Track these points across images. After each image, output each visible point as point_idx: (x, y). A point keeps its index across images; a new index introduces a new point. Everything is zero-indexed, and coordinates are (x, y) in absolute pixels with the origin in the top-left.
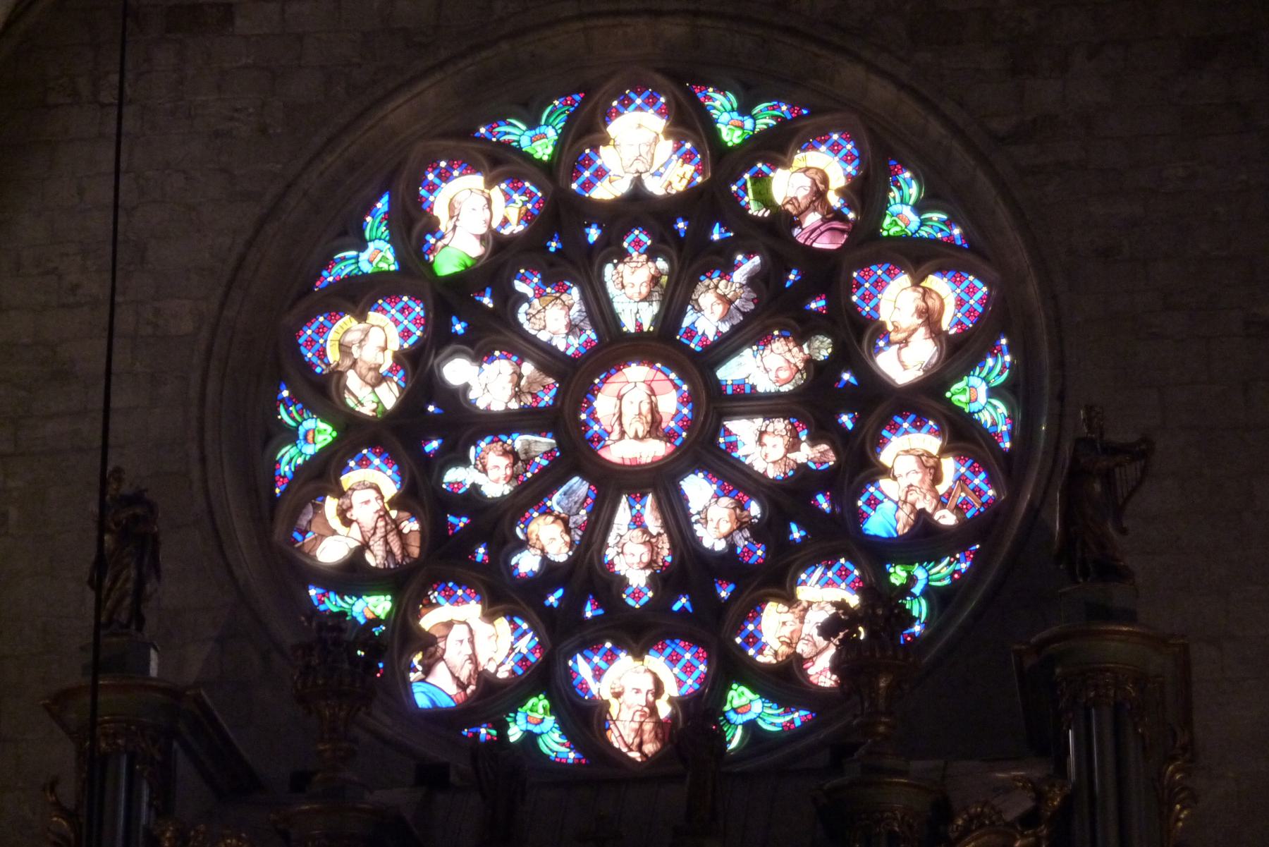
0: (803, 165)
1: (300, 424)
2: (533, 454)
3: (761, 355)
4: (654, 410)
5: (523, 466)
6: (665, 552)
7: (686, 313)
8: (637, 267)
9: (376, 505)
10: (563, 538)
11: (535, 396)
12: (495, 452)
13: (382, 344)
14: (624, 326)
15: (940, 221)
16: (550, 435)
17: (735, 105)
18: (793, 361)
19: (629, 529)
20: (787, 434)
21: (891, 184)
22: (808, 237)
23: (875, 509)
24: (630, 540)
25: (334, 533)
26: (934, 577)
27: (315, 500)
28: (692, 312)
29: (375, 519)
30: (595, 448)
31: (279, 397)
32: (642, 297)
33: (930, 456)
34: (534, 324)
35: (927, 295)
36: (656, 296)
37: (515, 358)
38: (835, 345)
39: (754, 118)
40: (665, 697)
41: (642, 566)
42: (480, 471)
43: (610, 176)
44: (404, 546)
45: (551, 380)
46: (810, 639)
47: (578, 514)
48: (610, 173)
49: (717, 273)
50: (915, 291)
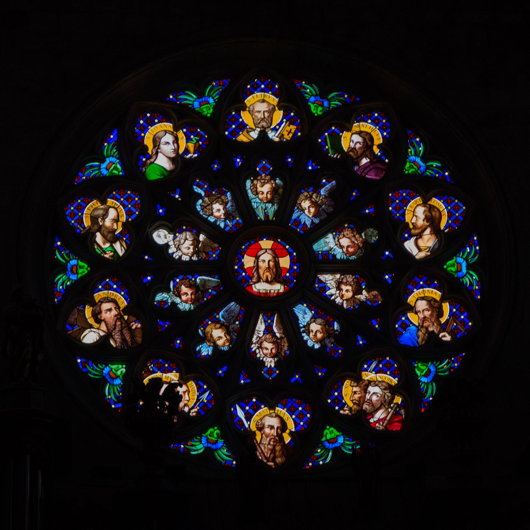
0: (358, 130)
1: (69, 262)
2: (208, 287)
3: (338, 238)
4: (277, 264)
5: (201, 293)
6: (286, 348)
7: (294, 211)
8: (264, 182)
9: (114, 312)
10: (226, 337)
11: (207, 254)
12: (184, 285)
13: (116, 218)
14: (258, 216)
15: (437, 166)
16: (217, 277)
17: (318, 92)
18: (356, 242)
19: (264, 334)
20: (354, 284)
21: (409, 144)
22: (363, 171)
23: (405, 330)
24: (265, 340)
25: (91, 327)
26: (440, 370)
27: (79, 307)
28: (297, 210)
29: (115, 320)
30: (244, 286)
31: (55, 245)
32: (268, 200)
33: (435, 300)
34: (206, 212)
35: (431, 209)
36: (276, 200)
37: (195, 231)
38: (379, 235)
39: (329, 101)
40: (288, 431)
41: (272, 355)
42: (176, 296)
43: (247, 128)
44: (133, 336)
45: (216, 245)
46: (370, 402)
47: (235, 323)
48: (248, 127)
49: (311, 189)
50: (424, 206)
